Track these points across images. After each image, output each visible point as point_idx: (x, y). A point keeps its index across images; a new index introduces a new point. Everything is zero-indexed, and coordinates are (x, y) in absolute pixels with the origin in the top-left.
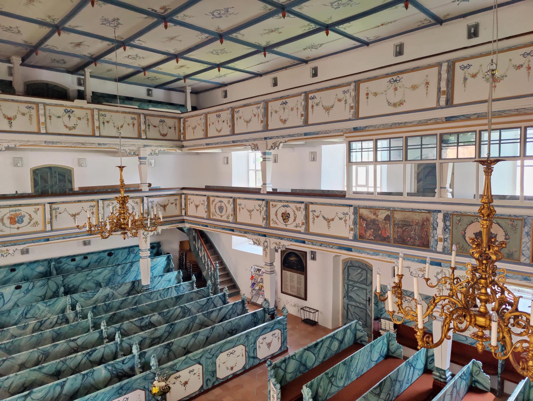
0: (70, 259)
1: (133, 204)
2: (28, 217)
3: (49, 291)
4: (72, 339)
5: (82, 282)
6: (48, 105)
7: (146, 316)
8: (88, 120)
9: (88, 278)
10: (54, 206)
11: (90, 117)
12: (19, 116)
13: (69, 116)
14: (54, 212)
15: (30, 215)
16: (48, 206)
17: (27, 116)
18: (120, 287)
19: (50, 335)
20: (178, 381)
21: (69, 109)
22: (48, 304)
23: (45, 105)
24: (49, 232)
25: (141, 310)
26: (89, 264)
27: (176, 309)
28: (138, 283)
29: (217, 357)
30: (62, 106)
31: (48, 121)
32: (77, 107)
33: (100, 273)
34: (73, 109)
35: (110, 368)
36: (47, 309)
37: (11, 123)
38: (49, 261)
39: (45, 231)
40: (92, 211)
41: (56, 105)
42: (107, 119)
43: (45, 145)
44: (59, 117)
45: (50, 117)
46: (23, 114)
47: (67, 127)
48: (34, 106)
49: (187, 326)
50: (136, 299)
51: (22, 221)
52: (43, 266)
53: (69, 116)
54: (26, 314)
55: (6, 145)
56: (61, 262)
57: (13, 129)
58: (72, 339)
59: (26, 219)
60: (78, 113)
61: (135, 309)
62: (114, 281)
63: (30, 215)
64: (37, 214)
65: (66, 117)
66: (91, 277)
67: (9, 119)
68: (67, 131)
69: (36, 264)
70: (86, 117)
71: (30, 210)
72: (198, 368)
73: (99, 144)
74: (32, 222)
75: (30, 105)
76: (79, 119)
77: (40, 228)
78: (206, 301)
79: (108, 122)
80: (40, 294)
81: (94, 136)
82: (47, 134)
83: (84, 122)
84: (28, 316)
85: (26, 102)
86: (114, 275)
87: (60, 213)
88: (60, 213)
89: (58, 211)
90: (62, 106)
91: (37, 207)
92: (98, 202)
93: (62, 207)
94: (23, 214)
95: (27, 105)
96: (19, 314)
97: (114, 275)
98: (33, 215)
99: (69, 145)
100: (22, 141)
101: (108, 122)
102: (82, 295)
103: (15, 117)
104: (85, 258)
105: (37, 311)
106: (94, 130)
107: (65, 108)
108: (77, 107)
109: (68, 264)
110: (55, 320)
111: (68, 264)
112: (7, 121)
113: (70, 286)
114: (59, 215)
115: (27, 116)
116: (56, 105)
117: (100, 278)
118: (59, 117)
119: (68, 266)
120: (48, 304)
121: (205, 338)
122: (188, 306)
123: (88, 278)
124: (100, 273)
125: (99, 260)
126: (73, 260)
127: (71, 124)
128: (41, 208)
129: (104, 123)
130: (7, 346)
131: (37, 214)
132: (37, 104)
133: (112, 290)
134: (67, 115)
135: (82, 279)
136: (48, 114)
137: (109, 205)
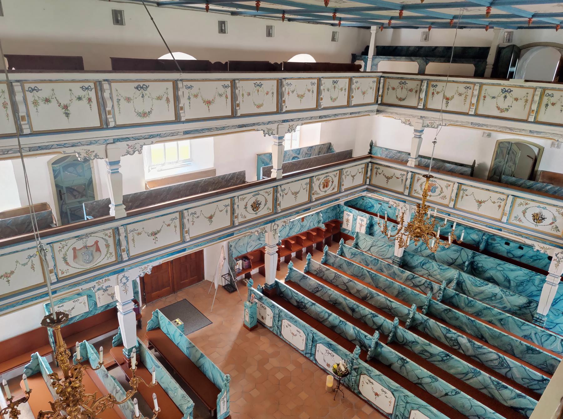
0: (504, 242)
1: (556, 214)
2: (440, 189)
3: (460, 258)
4: (389, 299)
5: (491, 268)
6: (485, 84)
7: (454, 331)
8: (526, 101)
9: (499, 268)
10: (463, 187)
11: (530, 99)
12: (456, 97)
13: (505, 97)
14: (462, 192)
15: (442, 188)
16: (456, 185)
17: (463, 96)
18: (511, 295)
19: (398, 288)
20: (370, 385)
21: (507, 88)
22: (441, 267)
23: (481, 85)
24: (451, 208)
25: (478, 326)
26: (522, 256)
27: (491, 352)
28: (535, 305)
29: (413, 409)
30: (499, 85)
31: (481, 101)
32: (515, 86)
33: (512, 270)
34: (512, 89)
35: (356, 332)
36: (439, 270)
37: (447, 103)
38: (484, 233)
39: (447, 206)
40: (499, 204)
41: (493, 84)
42: (553, 100)
43: (471, 126)
44: (494, 98)
45: (485, 97)
46: (460, 95)
47: (498, 108)
48: (472, 86)
49: (465, 371)
50: (502, 317)
51: (435, 192)
52: (478, 235)
53: (505, 97)
54: (423, 265)
55: (438, 123)
56: (495, 240)
57: (448, 109)
58: (389, 299)
59: (438, 191)
60: (517, 92)
61: (472, 321)
62: (527, 287)
63: (442, 188)
64: (447, 189)
65: (502, 98)
66: (502, 269)
67: (448, 99)
68: (497, 113)
69: (472, 231)
70: (525, 98)
71: (443, 184)
72: (389, 394)
73: (530, 131)
74: (442, 195)
75: (468, 85)
76: (516, 99)
77: (446, 202)
78: (541, 378)
79: (553, 104)
80: (452, 257)
81: (526, 121)
82: (476, 115)
83: (521, 103)
84: (424, 267)
85: (464, 82)
86: (529, 281)
87: (467, 195)
88: (467, 195)
89: (466, 193)
90: (499, 85)
91: (450, 183)
92: (508, 196)
93: (470, 190)
94: (437, 185)
95: (465, 85)
96: (419, 261)
97: (529, 281)
98: (444, 189)
99: (495, 129)
100: (451, 121)
101: (553, 104)
102: (471, 279)
103: (453, 97)
104: (521, 248)
105: (431, 268)
106: (529, 115)
107: (502, 88)
108: (515, 86)
109: (501, 245)
110: (423, 281)
111: (501, 245)
112: (445, 101)
113: (480, 265)
114: (465, 197)
115: (463, 96)
116: (493, 84)
117: (512, 275)
118: (494, 98)
119: (500, 247)
120: (441, 267)
121: (444, 393)
122: (508, 362)
123: (499, 268)
124: (512, 270)
125: (536, 258)
126: (507, 244)
127: (503, 106)
128: (452, 184)
129: (547, 105)
130: (373, 275)
131: (447, 189)
132: (474, 84)
133: (501, 293)
134: (504, 95)
135: (492, 265)
136: (483, 94)
137: (521, 204)
